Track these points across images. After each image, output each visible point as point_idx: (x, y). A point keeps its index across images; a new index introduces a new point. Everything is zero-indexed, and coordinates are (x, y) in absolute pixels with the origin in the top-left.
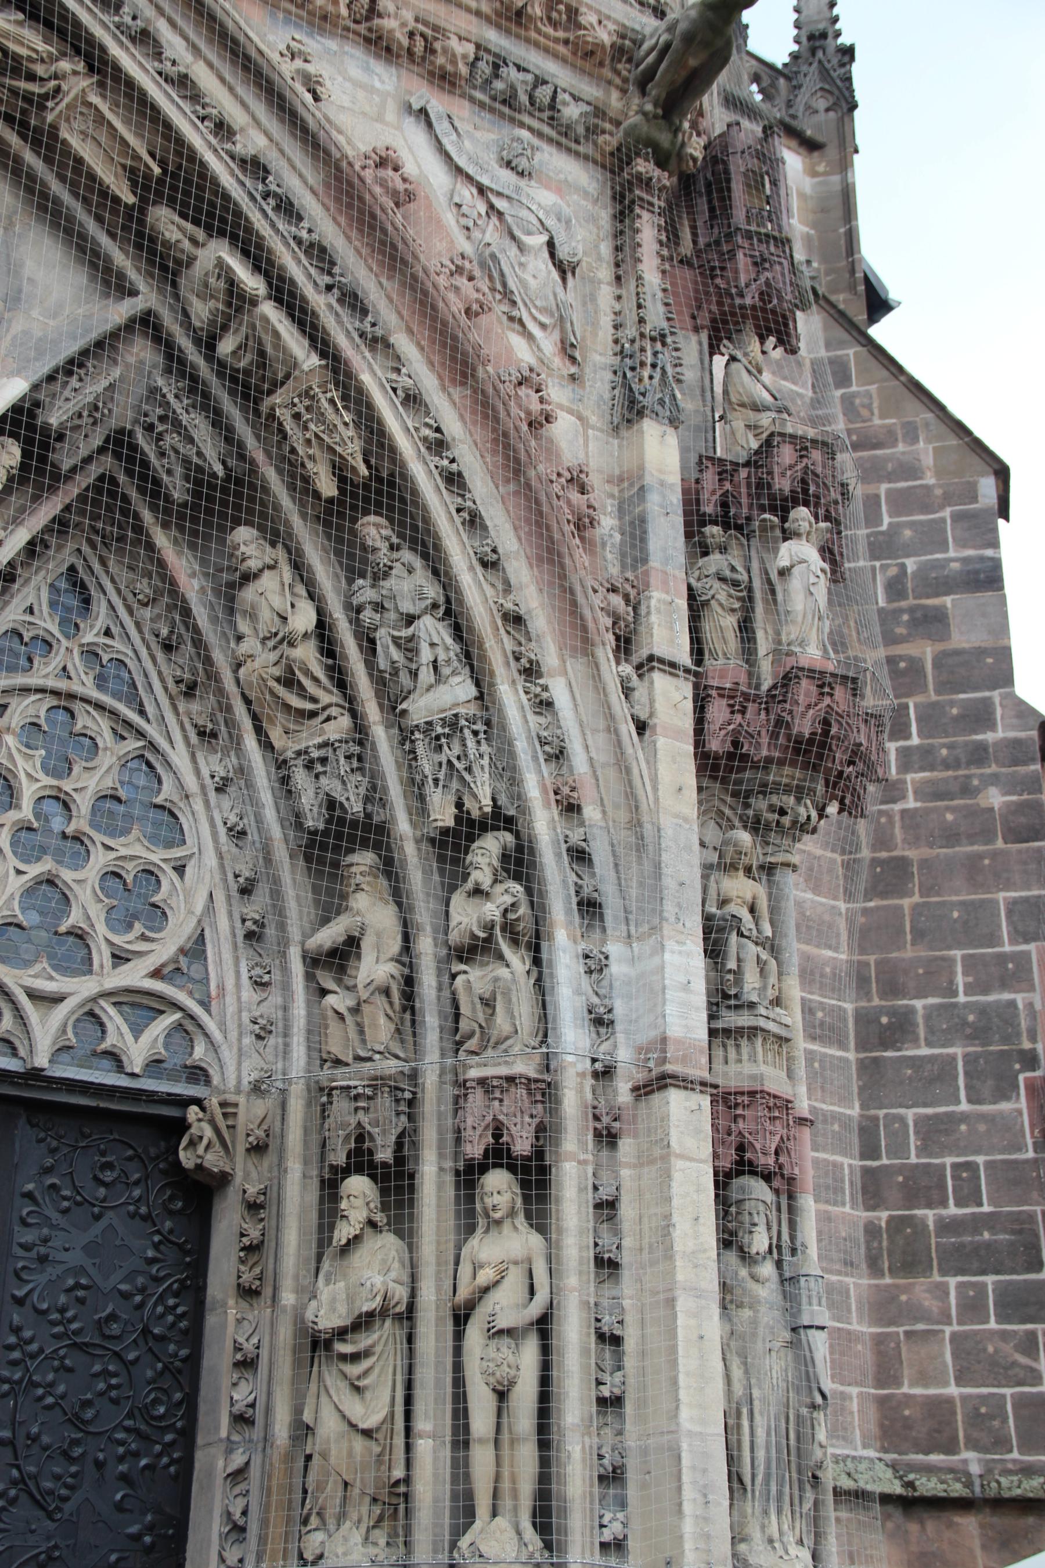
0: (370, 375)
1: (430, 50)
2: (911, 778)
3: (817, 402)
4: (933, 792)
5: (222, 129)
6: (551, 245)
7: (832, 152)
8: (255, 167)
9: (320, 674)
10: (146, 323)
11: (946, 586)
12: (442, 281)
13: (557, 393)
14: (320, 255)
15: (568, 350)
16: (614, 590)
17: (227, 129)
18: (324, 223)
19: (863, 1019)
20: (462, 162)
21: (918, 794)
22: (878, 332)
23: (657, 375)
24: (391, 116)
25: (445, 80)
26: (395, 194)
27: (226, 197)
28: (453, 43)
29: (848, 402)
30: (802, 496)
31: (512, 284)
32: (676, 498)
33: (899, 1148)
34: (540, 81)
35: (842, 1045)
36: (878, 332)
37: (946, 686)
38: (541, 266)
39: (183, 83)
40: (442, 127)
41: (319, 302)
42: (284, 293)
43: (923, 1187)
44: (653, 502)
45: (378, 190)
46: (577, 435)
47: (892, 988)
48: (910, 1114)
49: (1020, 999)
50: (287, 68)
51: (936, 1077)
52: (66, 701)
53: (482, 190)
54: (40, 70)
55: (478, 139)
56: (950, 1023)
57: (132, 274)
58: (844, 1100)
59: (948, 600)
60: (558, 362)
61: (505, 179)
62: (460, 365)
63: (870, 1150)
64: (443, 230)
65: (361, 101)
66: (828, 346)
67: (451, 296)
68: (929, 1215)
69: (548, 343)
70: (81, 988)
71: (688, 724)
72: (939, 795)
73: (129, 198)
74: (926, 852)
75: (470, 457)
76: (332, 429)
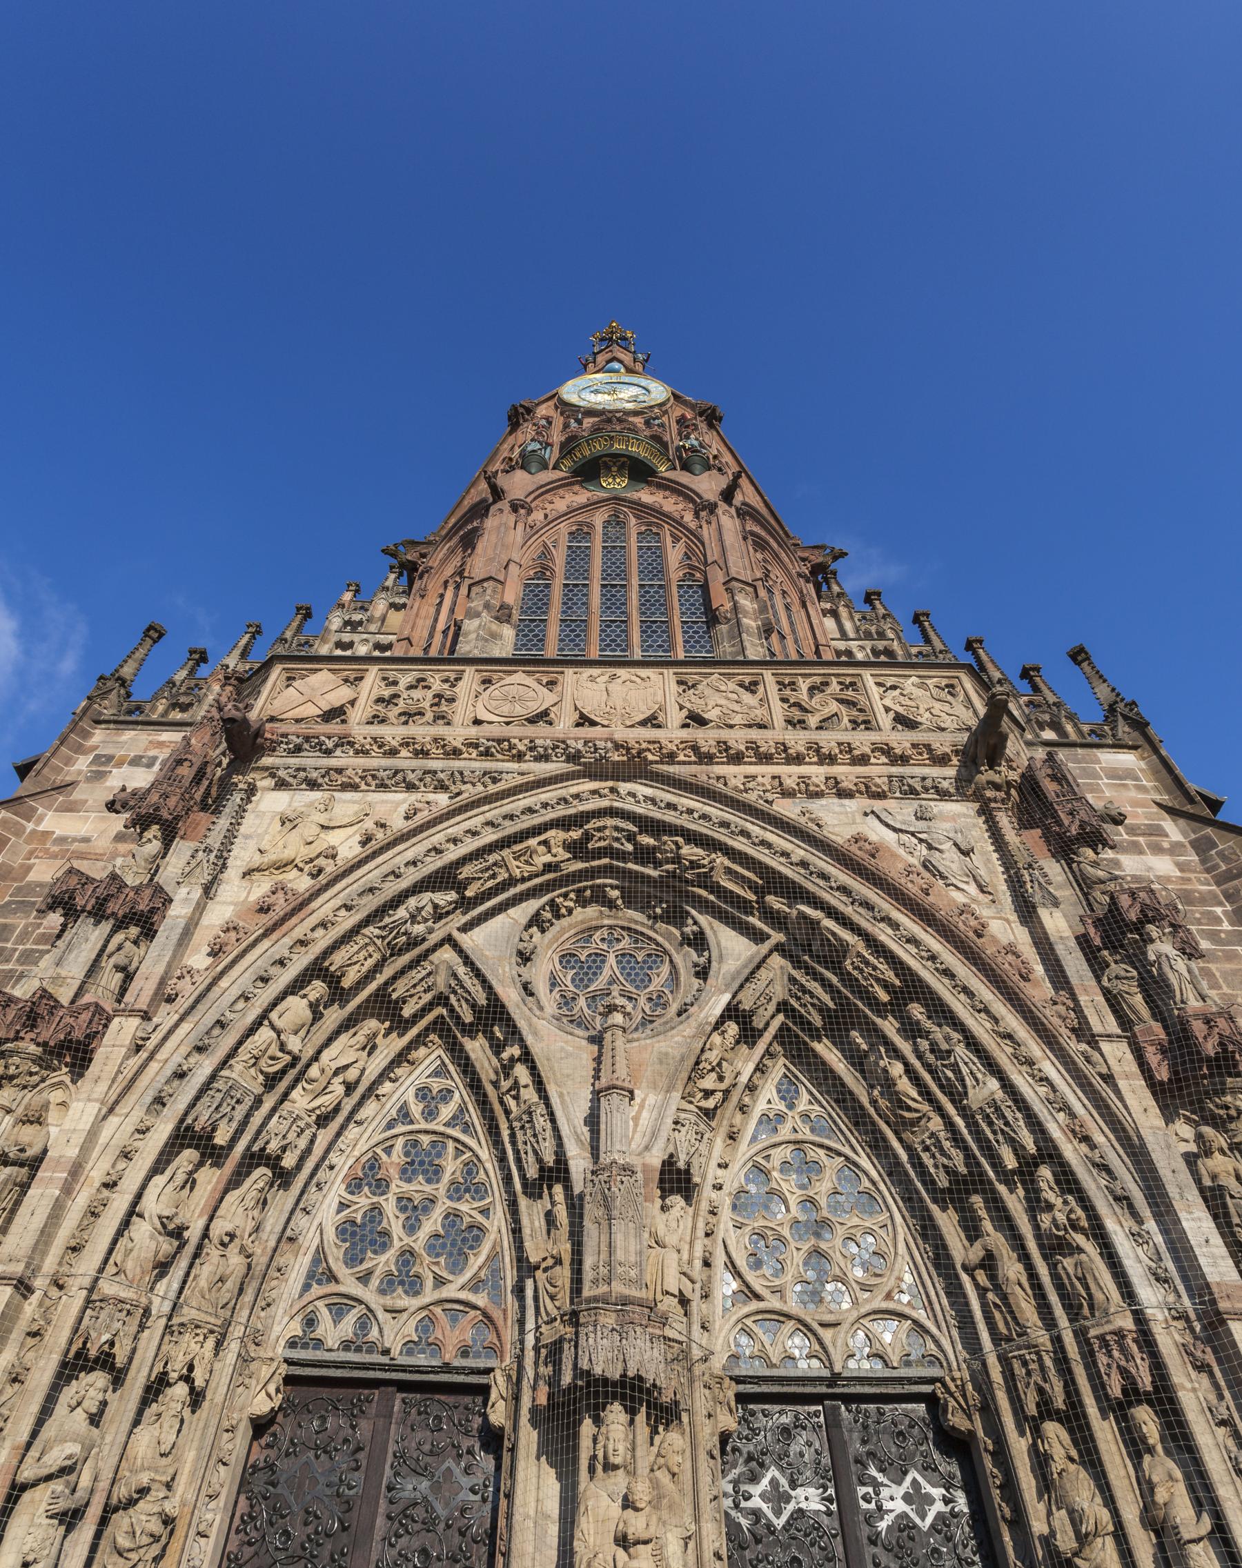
0: (884, 935)
1: (867, 787)
3: (1203, 862)
5: (785, 854)
6: (956, 844)
8: (804, 864)
9: (914, 1094)
12: (903, 881)
13: (985, 912)
14: (844, 889)
15: (982, 889)
16: (1055, 1003)
17: (784, 855)
18: (841, 876)
20: (898, 826)
22: (1220, 817)
23: (1036, 886)
24: (859, 818)
25: (881, 796)
26: (866, 852)
27: (794, 882)
28: (878, 780)
29: (1221, 854)
30: (1145, 919)
31: (941, 869)
32: (1073, 943)
34: (924, 779)
36: (1220, 817)
38: (954, 854)
39: (764, 843)
40: (883, 816)
41: (848, 910)
42: (832, 913)
44: (1060, 950)
45: (859, 853)
50: (803, 820)
53: (913, 834)
54: (705, 862)
55: (902, 811)
57: (766, 929)
60: (981, 896)
61: (921, 825)
62: (926, 916)
64: (900, 856)
65: (840, 819)
67: (910, 885)
69: (972, 889)
71: (1134, 1068)
73: (754, 898)
75: (950, 958)
76: (875, 968)
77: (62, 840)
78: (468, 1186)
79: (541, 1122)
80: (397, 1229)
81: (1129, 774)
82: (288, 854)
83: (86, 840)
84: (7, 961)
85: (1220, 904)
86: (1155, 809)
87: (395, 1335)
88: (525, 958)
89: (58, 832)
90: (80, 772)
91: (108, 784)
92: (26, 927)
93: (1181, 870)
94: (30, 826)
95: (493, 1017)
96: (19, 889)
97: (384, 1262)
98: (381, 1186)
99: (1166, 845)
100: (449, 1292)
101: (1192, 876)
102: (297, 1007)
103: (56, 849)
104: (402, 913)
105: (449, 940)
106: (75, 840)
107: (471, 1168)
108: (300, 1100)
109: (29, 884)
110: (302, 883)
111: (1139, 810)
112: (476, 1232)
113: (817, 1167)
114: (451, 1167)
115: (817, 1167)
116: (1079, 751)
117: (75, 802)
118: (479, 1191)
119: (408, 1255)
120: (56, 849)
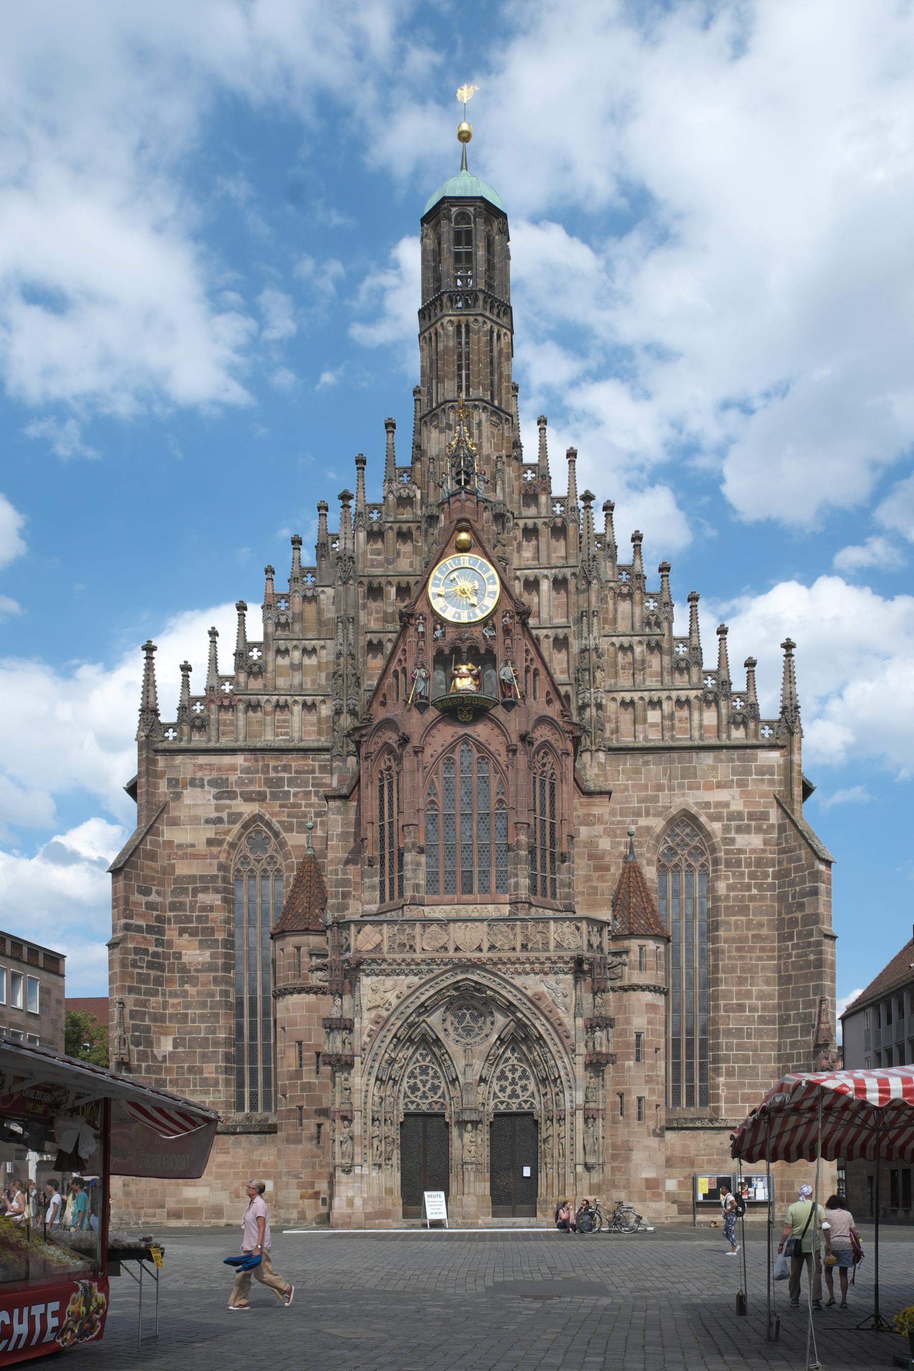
2: (794, 952)
3: (779, 838)
4: (798, 956)
7: (788, 747)
10: (512, 1020)
11: (803, 895)
19: (780, 1017)
21: (796, 957)
33: (785, 1049)
35: (774, 1024)
37: (804, 925)
43: (790, 1058)
46: (568, 1020)
47: (787, 1009)
48: (788, 1040)
49: (813, 1011)
51: (794, 1031)
52: (513, 1066)
56: (798, 1017)
58: (774, 1038)
59: (805, 899)
63: (779, 1050)
66: (782, 819)
68: (790, 1064)
70: (518, 1101)
72: (799, 957)
74: (796, 973)
77: (180, 846)
78: (435, 1076)
79: (452, 1069)
80: (421, 1087)
81: (770, 770)
82: (377, 1003)
83: (193, 846)
84: (192, 922)
85: (774, 866)
86: (772, 799)
87: (424, 1108)
88: (444, 1020)
89: (176, 842)
90: (165, 793)
91: (185, 803)
92: (191, 902)
93: (765, 845)
94: (161, 839)
95: (437, 1041)
96: (174, 879)
97: (420, 1094)
98: (415, 1078)
99: (765, 827)
100: (434, 1099)
101: (768, 848)
102: (392, 1046)
103: (180, 852)
104: (412, 1019)
105: (424, 1021)
106: (187, 846)
107: (436, 1072)
108: (396, 1066)
109: (178, 877)
110: (385, 1014)
111: (762, 800)
112: (439, 1087)
113: (517, 1070)
114: (431, 1073)
115: (517, 1070)
116: (748, 751)
117: (174, 818)
118: (438, 1078)
119: (424, 1092)
120: (180, 852)
